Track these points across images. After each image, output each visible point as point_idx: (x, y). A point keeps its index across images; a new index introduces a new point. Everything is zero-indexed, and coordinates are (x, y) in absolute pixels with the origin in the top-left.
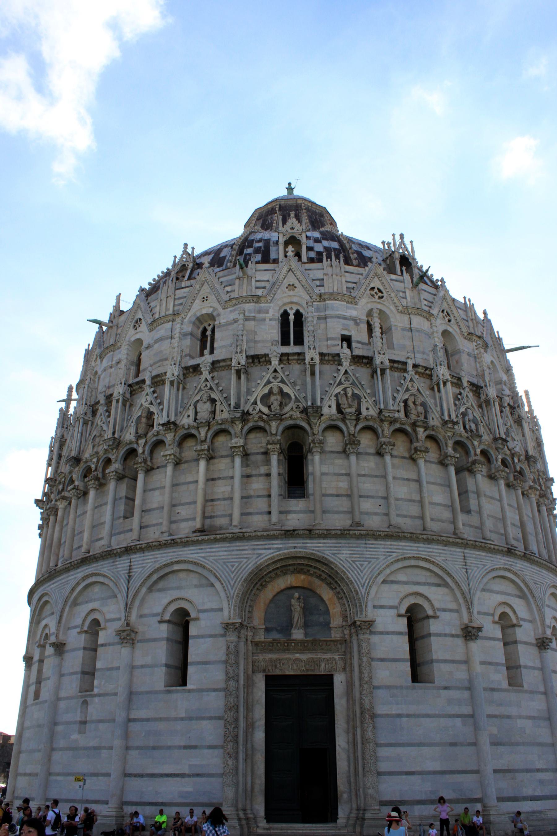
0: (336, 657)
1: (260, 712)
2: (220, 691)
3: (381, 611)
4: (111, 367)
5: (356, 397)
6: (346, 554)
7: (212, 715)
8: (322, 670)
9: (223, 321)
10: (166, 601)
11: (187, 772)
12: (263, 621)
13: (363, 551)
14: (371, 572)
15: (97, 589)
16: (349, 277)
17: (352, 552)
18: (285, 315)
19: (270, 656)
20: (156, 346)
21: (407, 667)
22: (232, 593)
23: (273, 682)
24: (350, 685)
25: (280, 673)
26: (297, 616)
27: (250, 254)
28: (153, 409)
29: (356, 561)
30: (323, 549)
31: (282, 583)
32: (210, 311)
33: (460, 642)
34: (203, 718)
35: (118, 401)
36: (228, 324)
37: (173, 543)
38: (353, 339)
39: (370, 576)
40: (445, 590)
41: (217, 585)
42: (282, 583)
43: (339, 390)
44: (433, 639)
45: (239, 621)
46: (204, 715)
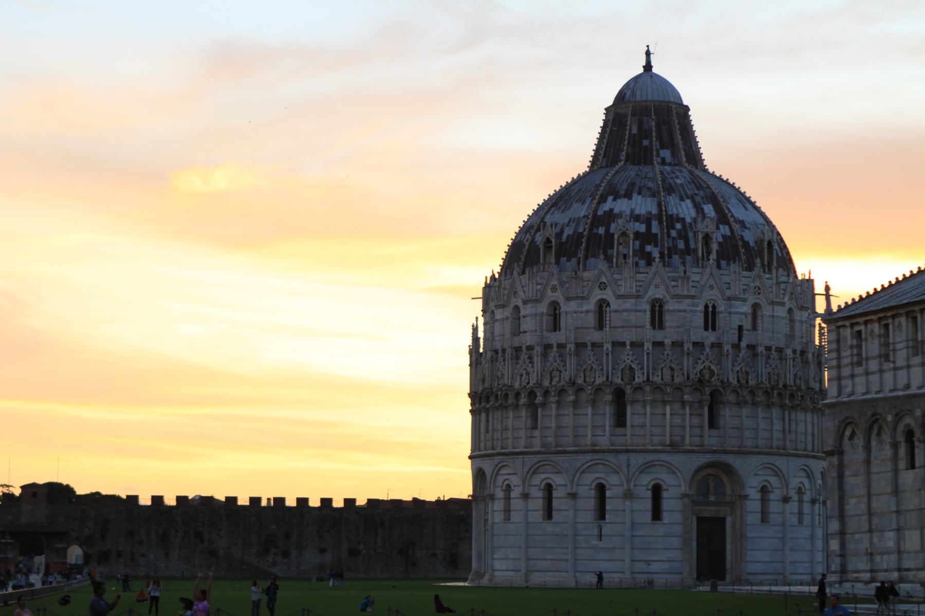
1: (694, 534)
3: (751, 489)
4: (582, 312)
5: (747, 373)
8: (722, 515)
9: (671, 308)
10: (649, 479)
11: (665, 559)
15: (600, 467)
16: (745, 281)
18: (706, 307)
19: (699, 508)
20: (625, 314)
21: (759, 515)
23: (700, 520)
24: (734, 523)
26: (712, 489)
27: (674, 238)
28: (633, 366)
31: (705, 472)
32: (661, 297)
33: (781, 503)
35: (607, 354)
36: (674, 311)
37: (656, 451)
38: (745, 327)
40: (776, 478)
41: (679, 474)
42: (705, 472)
43: (738, 368)
44: (771, 503)
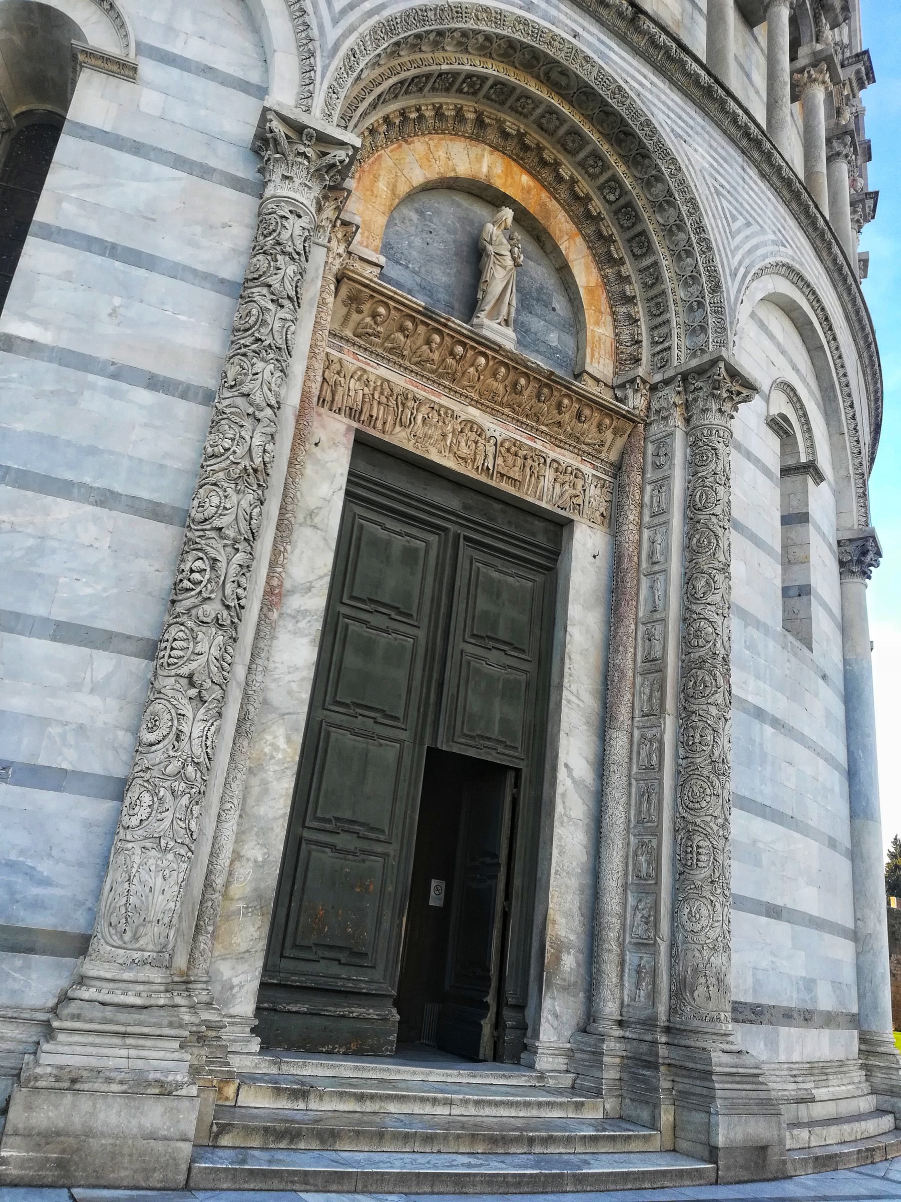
0: (587, 469)
2: (184, 396)
6: (703, 158)
7: (117, 488)
8: (544, 493)
12: (378, 243)
13: (738, 184)
14: (750, 252)
17: (715, 165)
22: (332, 34)
25: (410, 447)
29: (723, 196)
30: (650, 97)
34: (64, 489)
39: (747, 262)
45: (358, 143)
46: (68, 476)
